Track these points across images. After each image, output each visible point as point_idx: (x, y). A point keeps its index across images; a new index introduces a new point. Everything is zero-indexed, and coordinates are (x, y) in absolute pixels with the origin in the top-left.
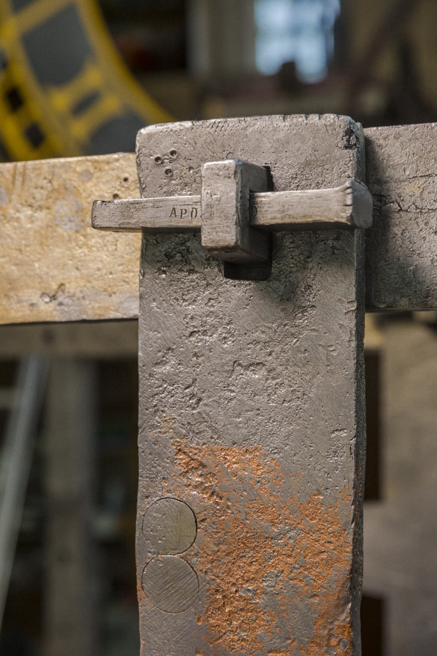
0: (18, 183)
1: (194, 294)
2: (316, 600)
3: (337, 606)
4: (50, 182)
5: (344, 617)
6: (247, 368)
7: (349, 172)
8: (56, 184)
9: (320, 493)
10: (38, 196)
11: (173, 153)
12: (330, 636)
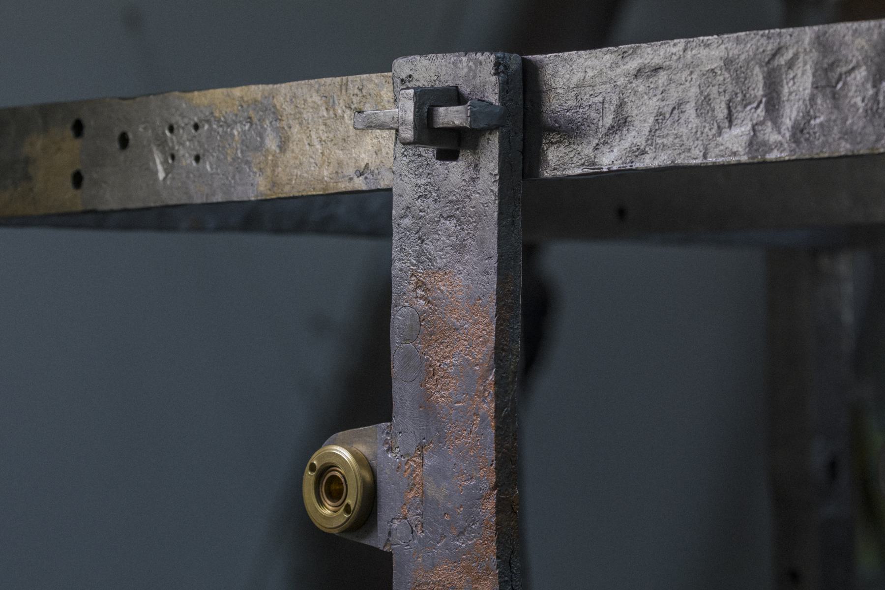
0: (344, 91)
1: (421, 170)
2: (477, 368)
3: (487, 371)
4: (361, 90)
5: (491, 377)
6: (446, 219)
7: (497, 91)
8: (364, 91)
9: (480, 299)
10: (355, 101)
11: (410, 76)
12: (485, 390)
